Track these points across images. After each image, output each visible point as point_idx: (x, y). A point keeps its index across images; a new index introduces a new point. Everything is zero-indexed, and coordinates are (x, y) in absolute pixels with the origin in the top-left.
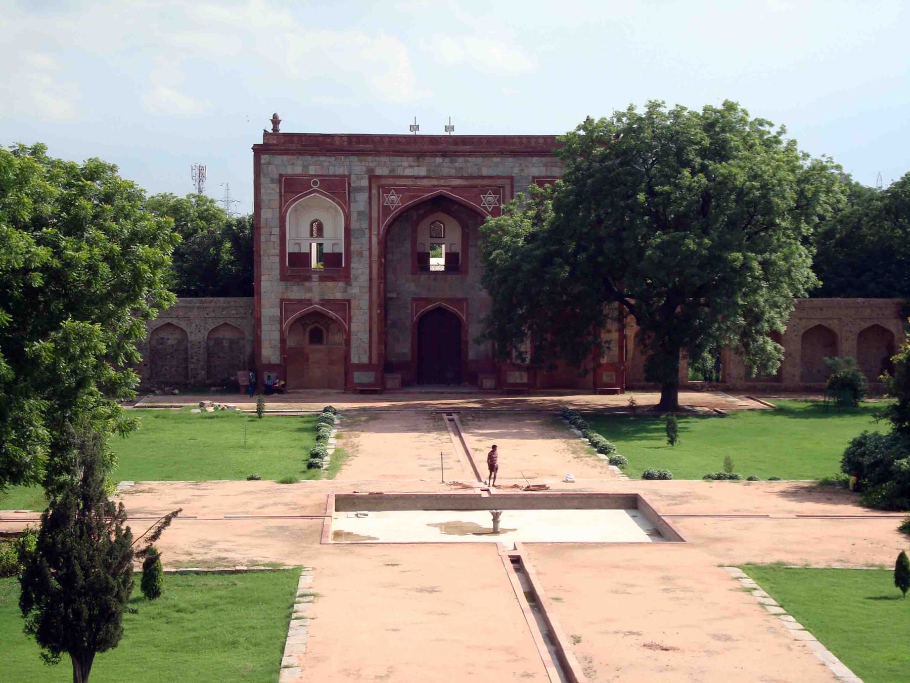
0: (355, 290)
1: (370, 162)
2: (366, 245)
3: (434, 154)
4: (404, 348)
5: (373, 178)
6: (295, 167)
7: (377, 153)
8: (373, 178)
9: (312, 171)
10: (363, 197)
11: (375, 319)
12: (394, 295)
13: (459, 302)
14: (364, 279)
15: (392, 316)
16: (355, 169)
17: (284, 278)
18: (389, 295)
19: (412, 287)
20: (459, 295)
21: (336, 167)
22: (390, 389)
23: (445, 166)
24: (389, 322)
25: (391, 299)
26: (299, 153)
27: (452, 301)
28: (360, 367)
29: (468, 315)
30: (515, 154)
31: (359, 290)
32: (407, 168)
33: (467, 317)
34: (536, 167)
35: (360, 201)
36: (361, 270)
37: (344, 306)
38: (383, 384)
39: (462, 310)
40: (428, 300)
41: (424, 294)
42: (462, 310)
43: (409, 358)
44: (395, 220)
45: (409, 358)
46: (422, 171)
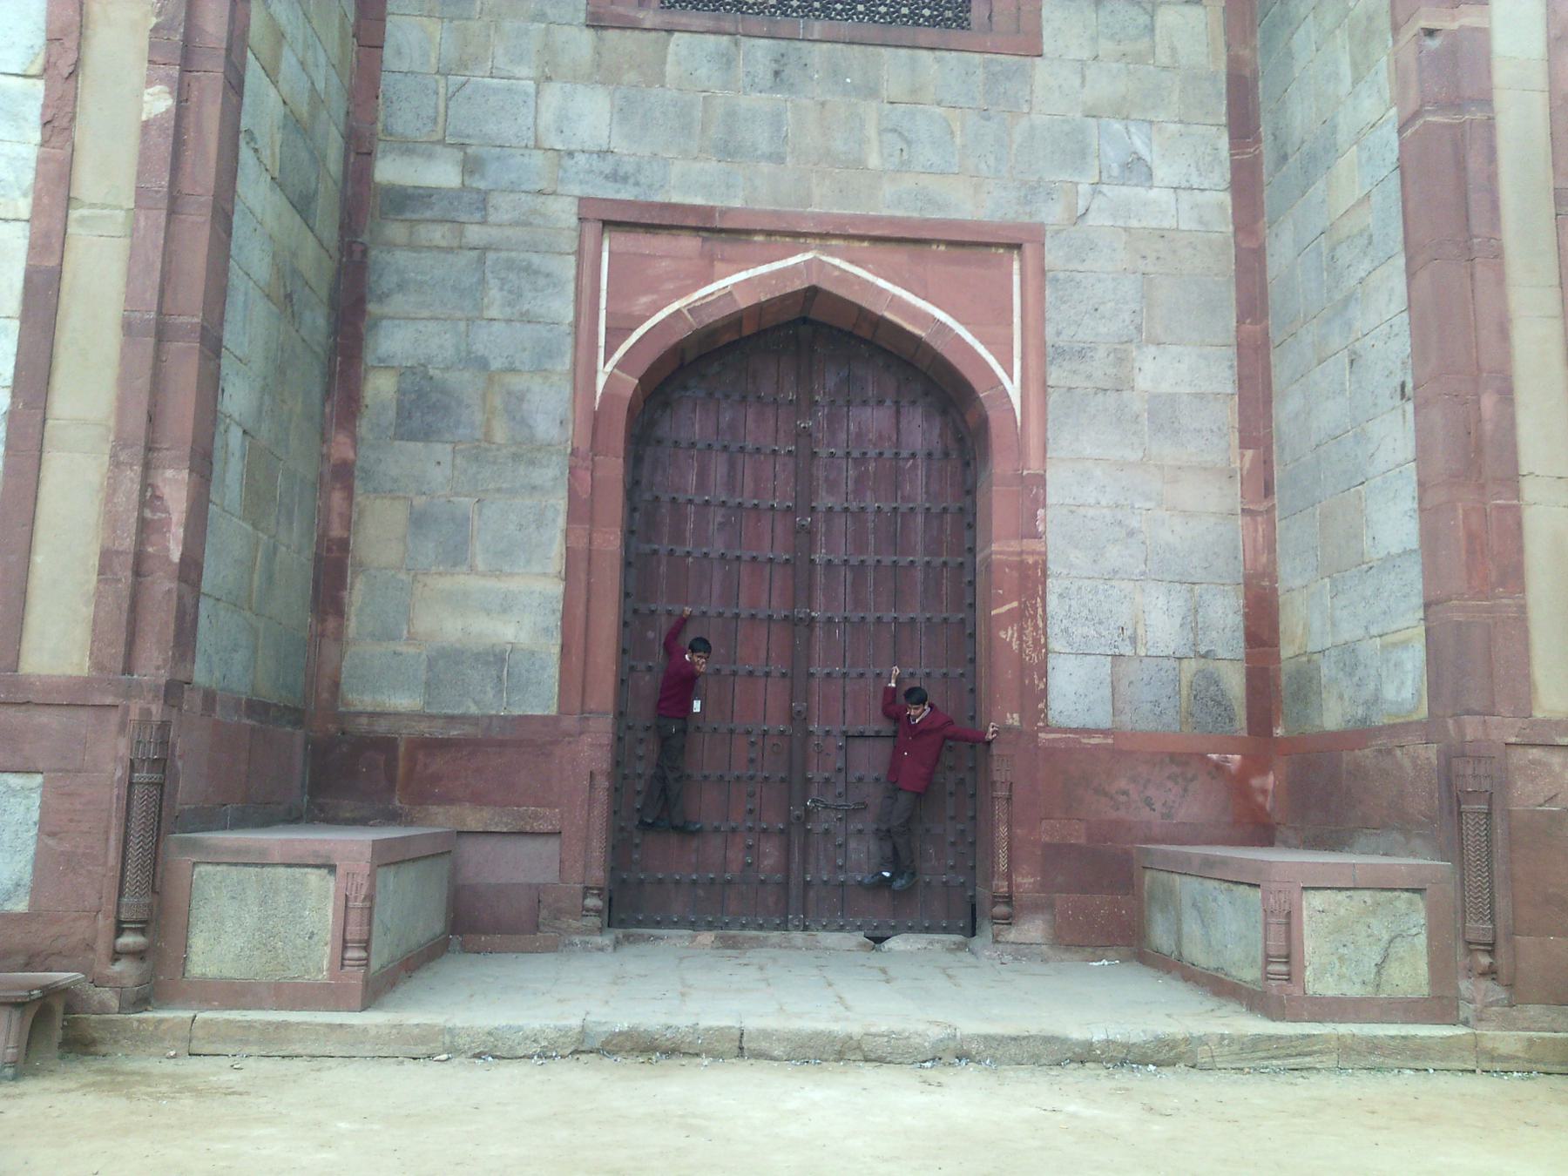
4: (493, 602)
11: (110, 174)
12: (442, 174)
15: (400, 340)
18: (389, 170)
19: (588, 116)
20: (971, 203)
22: (235, 993)
24: (380, 388)
25: (404, 200)
27: (902, 241)
29: (1040, 355)
33: (1038, 386)
38: (152, 924)
39: (992, 319)
40: (718, 232)
41: (688, 183)
42: (992, 319)
43: (541, 697)
45: (541, 697)
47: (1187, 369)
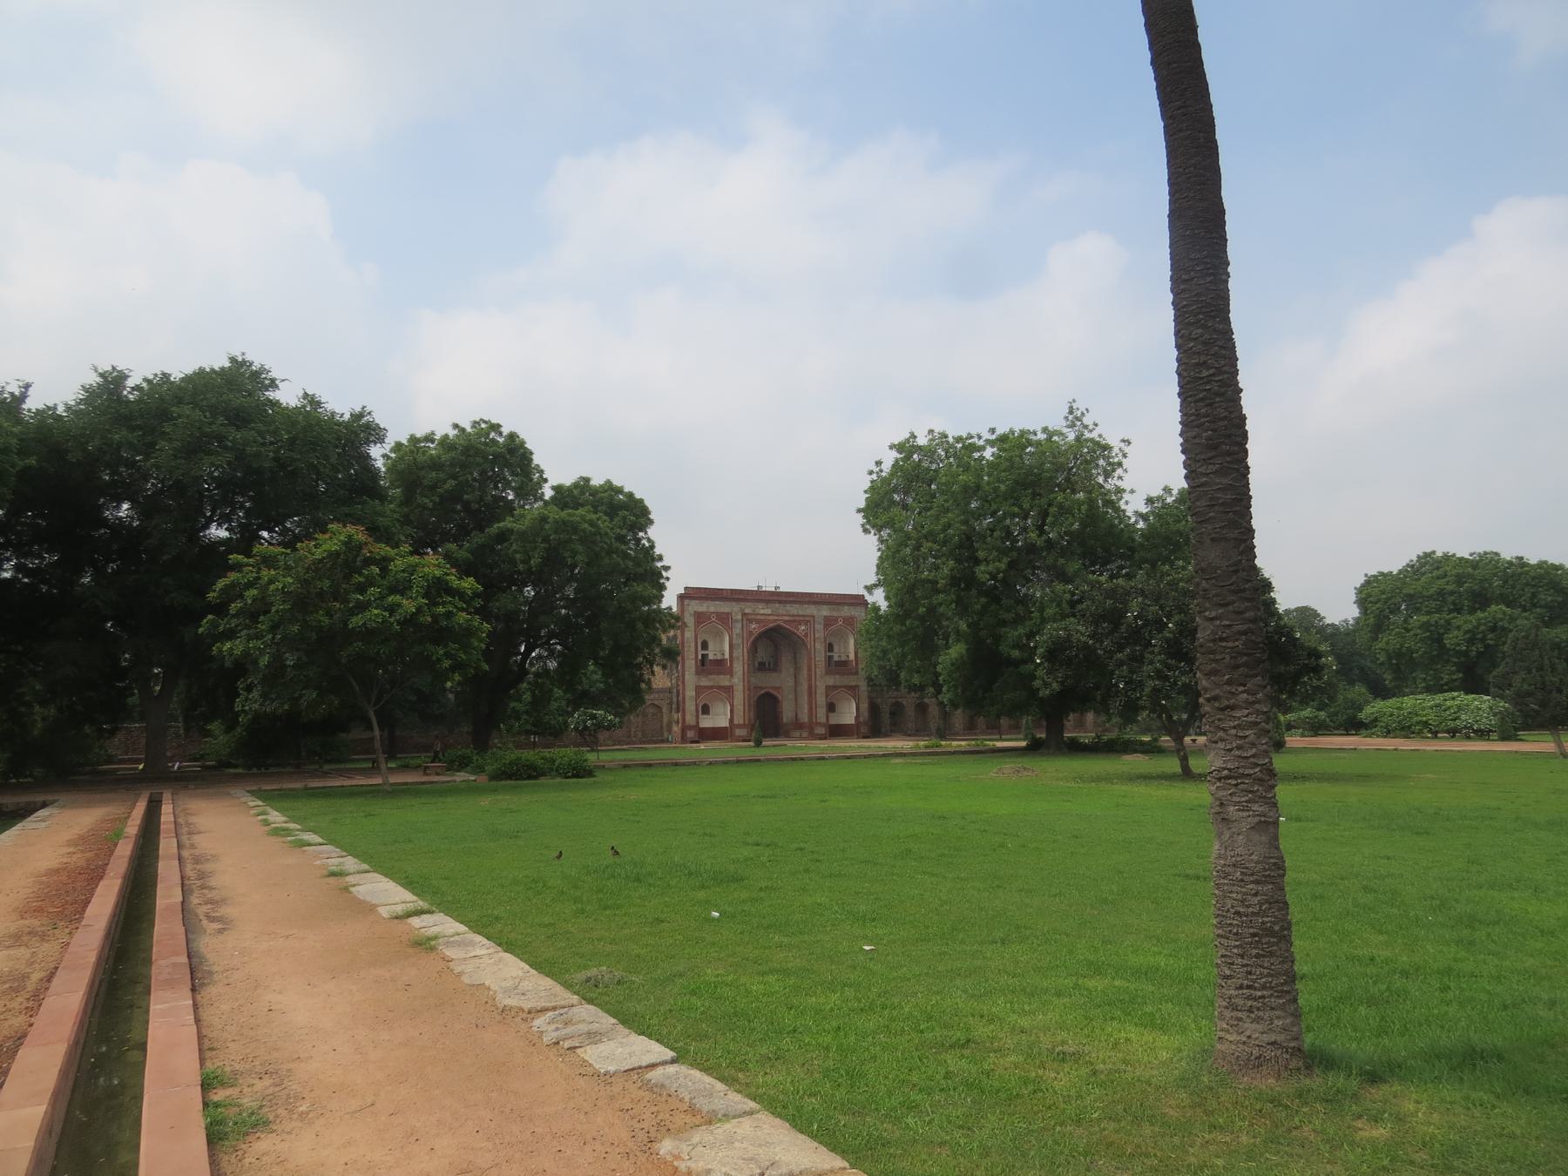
0: (735, 680)
1: (742, 605)
2: (742, 652)
3: (774, 602)
5: (744, 614)
6: (702, 607)
7: (745, 600)
8: (744, 614)
9: (712, 609)
10: (739, 625)
13: (778, 688)
14: (740, 673)
16: (734, 609)
17: (697, 673)
21: (724, 607)
23: (782, 609)
26: (706, 599)
28: (739, 726)
30: (815, 603)
31: (737, 680)
32: (763, 610)
34: (825, 611)
35: (737, 628)
36: (739, 668)
37: (729, 690)
44: (757, 639)
46: (769, 611)
47: (792, 697)
